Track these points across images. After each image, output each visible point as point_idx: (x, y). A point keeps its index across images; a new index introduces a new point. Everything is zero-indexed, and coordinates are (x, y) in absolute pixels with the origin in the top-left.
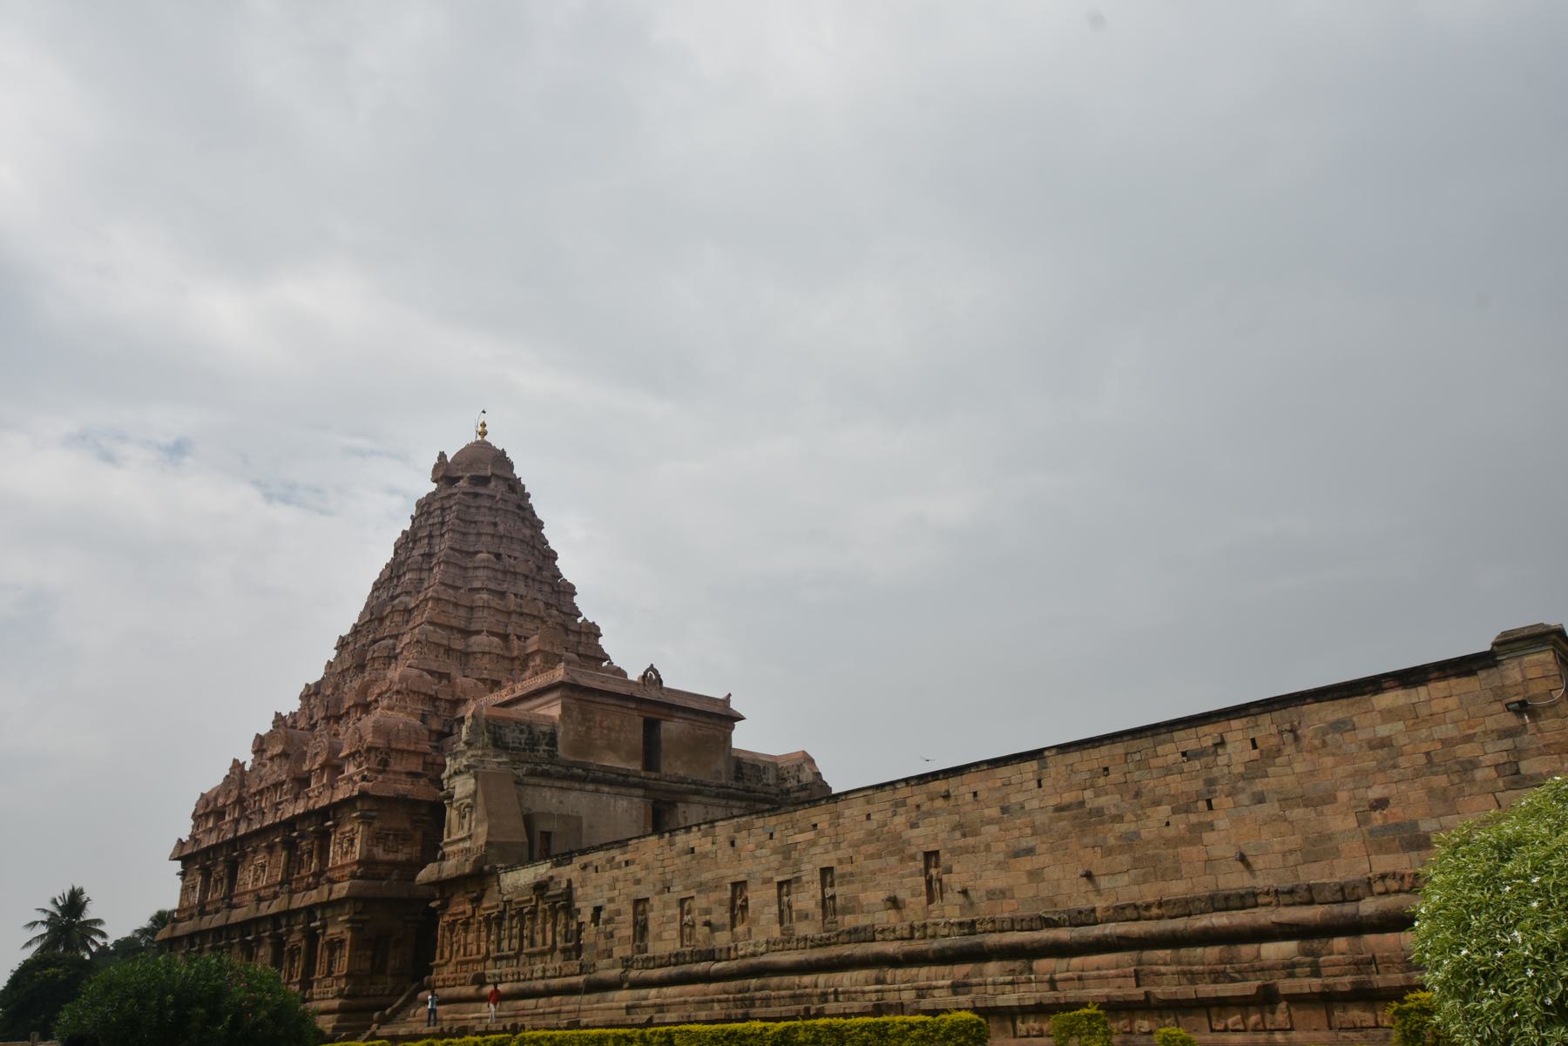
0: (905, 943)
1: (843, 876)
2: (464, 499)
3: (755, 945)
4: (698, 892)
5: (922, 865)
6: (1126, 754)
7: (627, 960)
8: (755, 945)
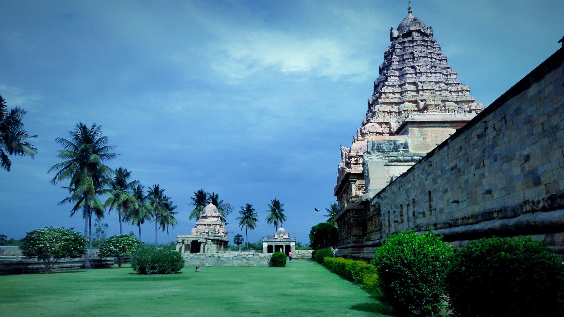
6: (465, 139)
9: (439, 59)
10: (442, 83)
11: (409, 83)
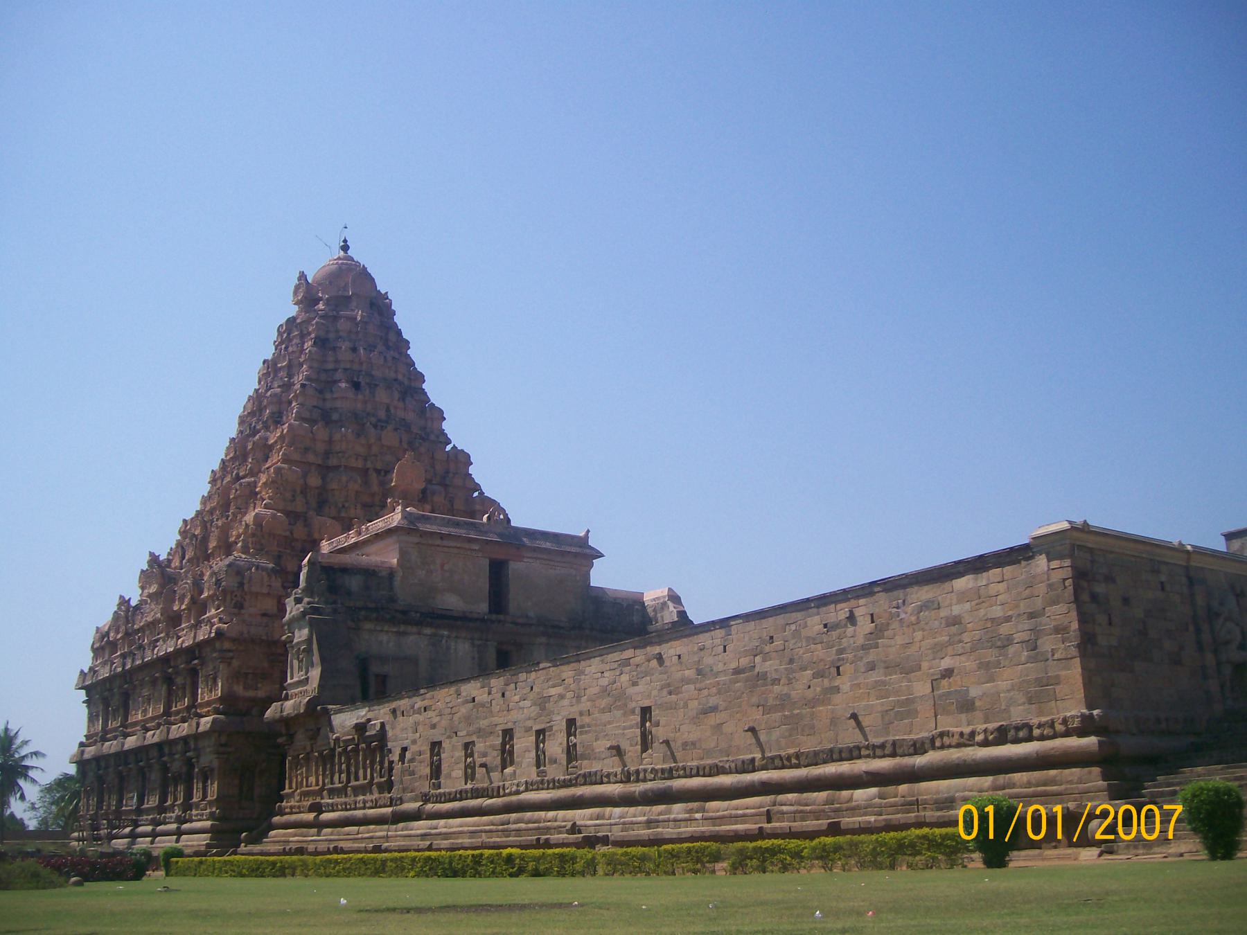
1: (582, 726)
3: (518, 786)
5: (639, 719)
7: (426, 795)
8: (518, 786)
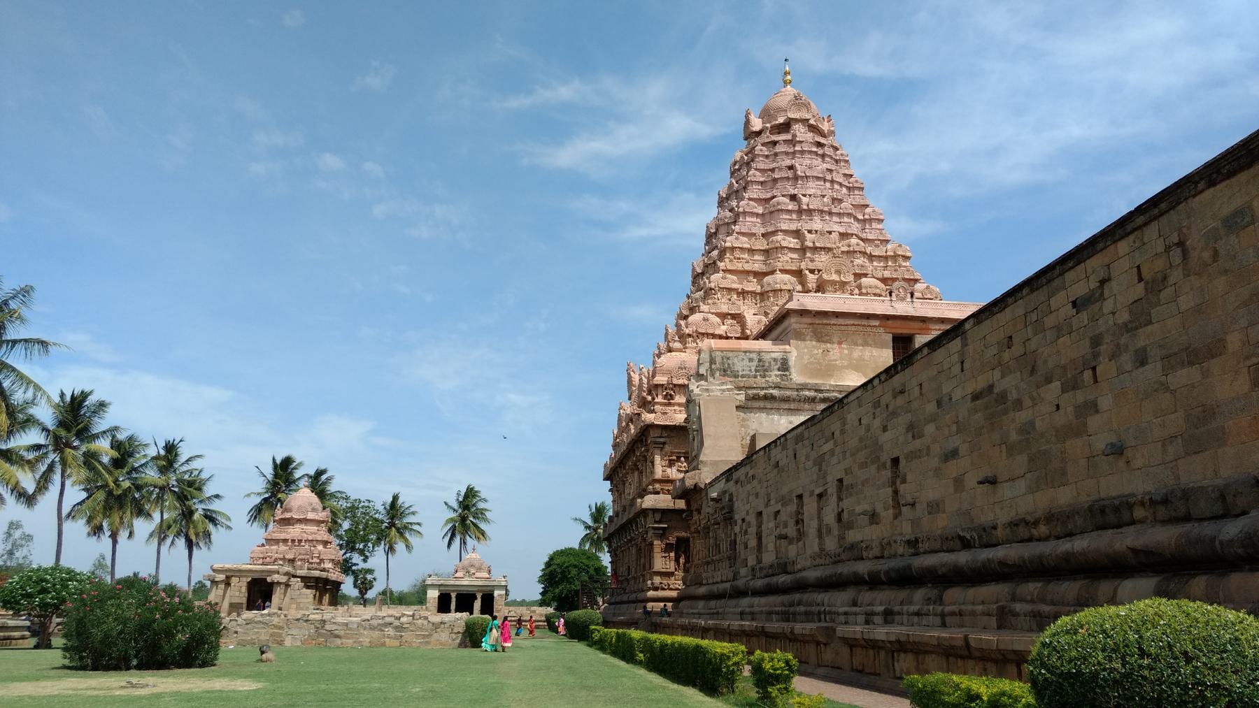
0: (875, 561)
2: (761, 150)
4: (782, 505)
5: (889, 475)
6: (1025, 315)
9: (848, 185)
10: (854, 237)
11: (785, 232)
